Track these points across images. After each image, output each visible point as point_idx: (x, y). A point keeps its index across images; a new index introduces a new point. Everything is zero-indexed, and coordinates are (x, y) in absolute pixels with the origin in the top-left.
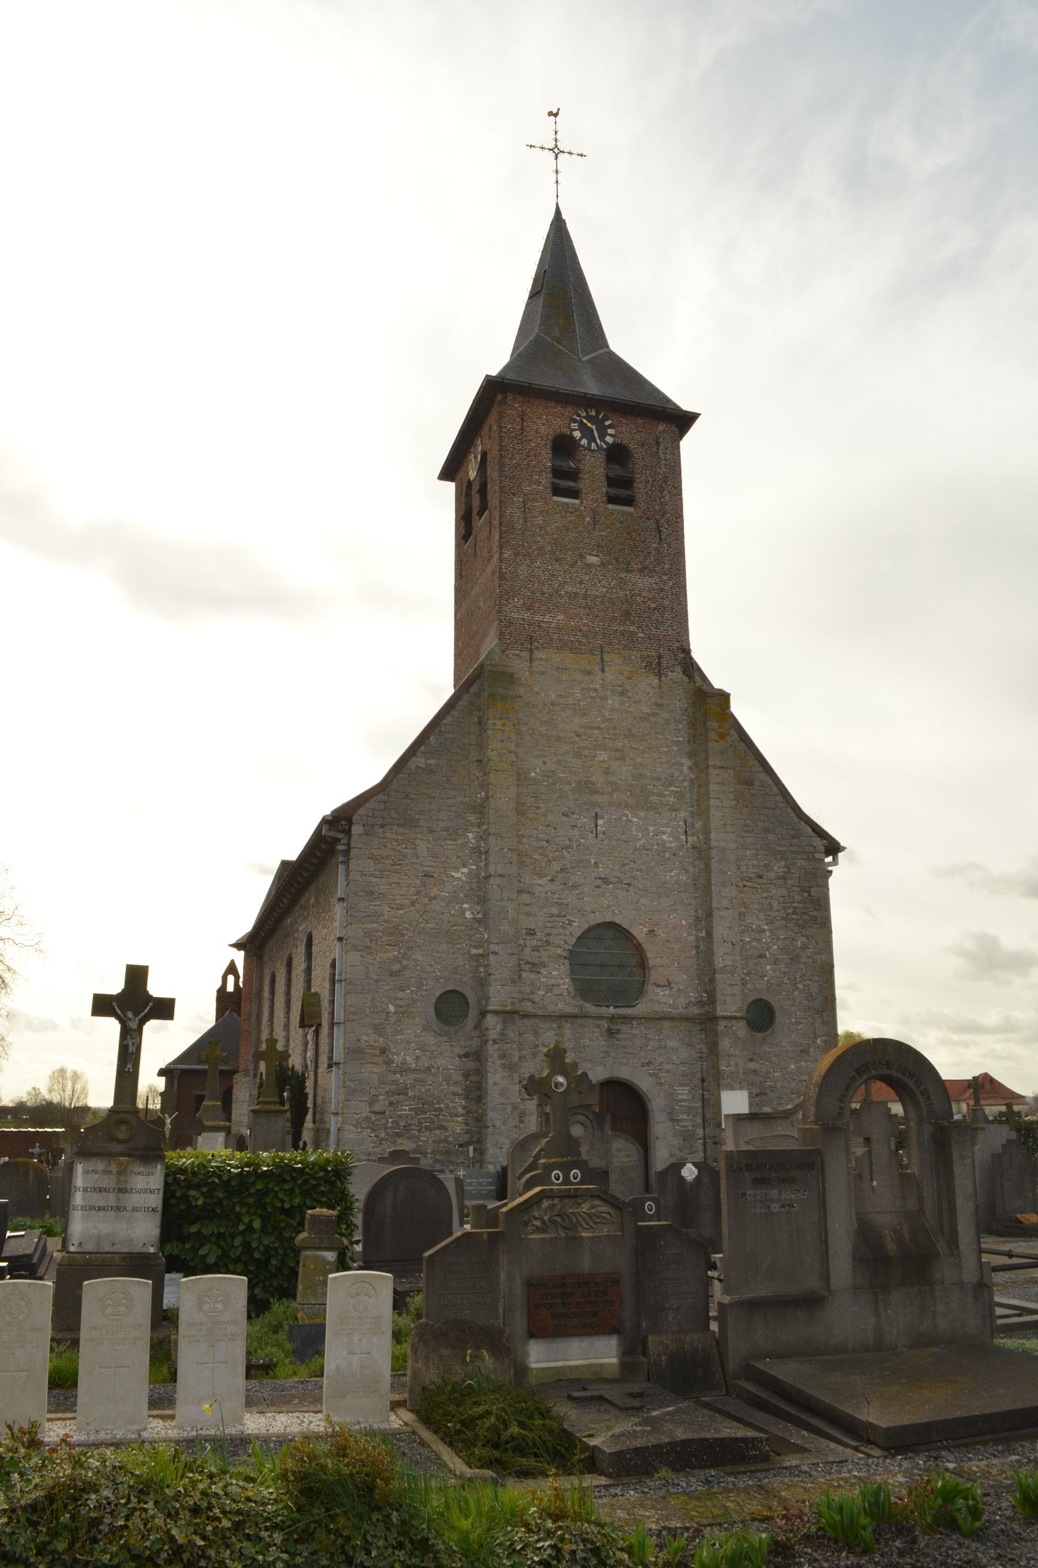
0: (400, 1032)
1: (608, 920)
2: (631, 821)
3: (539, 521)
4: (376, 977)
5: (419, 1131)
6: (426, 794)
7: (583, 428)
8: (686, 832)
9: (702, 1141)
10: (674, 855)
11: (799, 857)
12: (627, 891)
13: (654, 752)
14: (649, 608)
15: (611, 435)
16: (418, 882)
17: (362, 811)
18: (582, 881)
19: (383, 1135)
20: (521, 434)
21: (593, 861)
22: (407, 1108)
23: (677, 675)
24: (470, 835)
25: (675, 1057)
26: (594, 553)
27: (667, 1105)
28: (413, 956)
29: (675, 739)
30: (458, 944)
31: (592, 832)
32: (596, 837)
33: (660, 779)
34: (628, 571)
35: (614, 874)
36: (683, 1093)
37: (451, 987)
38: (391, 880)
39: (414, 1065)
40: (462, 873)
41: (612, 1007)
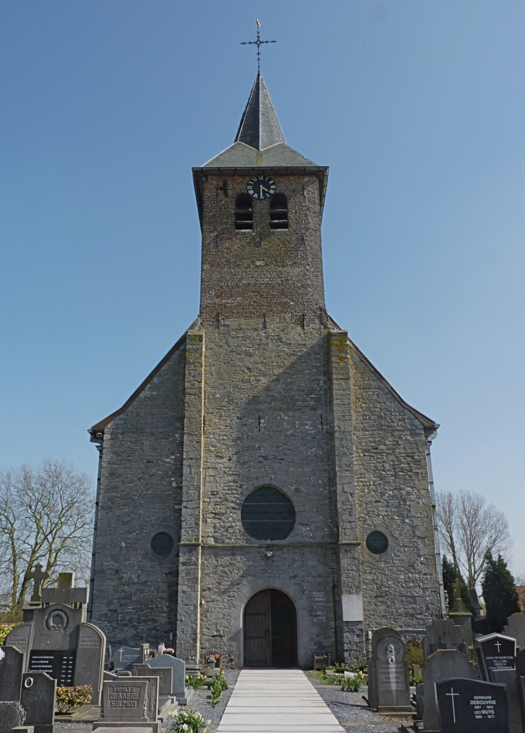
0: (128, 560)
1: (267, 483)
2: (283, 419)
4: (114, 526)
5: (139, 622)
6: (150, 412)
8: (322, 423)
9: (333, 630)
10: (314, 438)
11: (404, 433)
12: (280, 464)
13: (300, 374)
14: (297, 287)
15: (273, 189)
16: (143, 466)
18: (250, 459)
19: (115, 624)
20: (217, 197)
21: (257, 446)
22: (131, 608)
24: (177, 435)
25: (314, 572)
26: (261, 258)
27: (308, 605)
28: (138, 512)
29: (314, 364)
30: (166, 503)
31: (257, 428)
32: (259, 430)
33: (303, 391)
34: (283, 266)
35: (271, 453)
36: (319, 596)
37: (161, 531)
38: (126, 466)
39: (136, 580)
40: (171, 459)
41: (269, 540)
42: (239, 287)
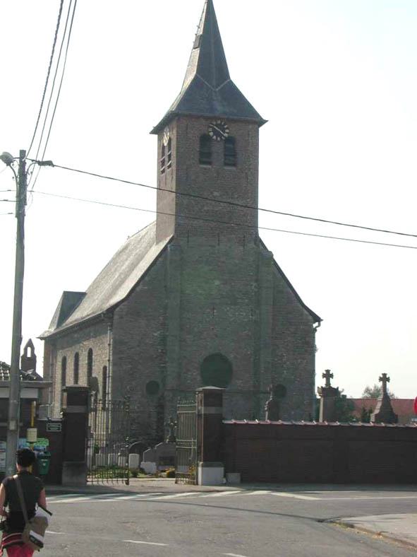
3: (193, 177)
7: (214, 131)
15: (227, 133)
17: (118, 309)
23: (252, 245)
42: (201, 212)
